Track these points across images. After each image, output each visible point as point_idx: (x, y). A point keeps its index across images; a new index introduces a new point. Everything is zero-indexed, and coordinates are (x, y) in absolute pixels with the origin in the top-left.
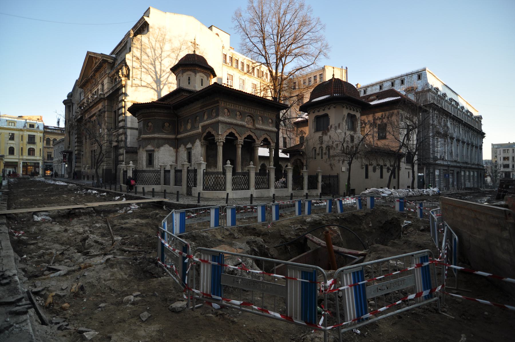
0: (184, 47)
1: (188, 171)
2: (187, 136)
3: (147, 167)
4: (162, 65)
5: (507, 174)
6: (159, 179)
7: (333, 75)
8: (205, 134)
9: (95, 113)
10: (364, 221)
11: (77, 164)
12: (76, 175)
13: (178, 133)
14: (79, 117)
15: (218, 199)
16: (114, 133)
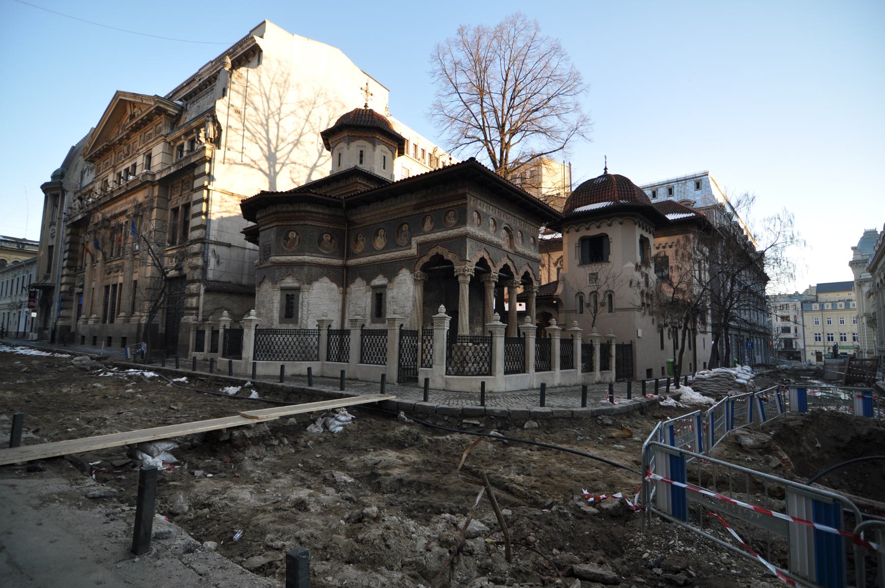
0: (321, 100)
1: (402, 333)
2: (374, 262)
3: (281, 321)
4: (280, 129)
5: (789, 342)
6: (318, 348)
7: (606, 169)
8: (426, 259)
9: (124, 212)
10: (804, 438)
11: (63, 313)
12: (65, 337)
13: (350, 255)
14: (80, 217)
15: (469, 396)
16: (170, 253)
